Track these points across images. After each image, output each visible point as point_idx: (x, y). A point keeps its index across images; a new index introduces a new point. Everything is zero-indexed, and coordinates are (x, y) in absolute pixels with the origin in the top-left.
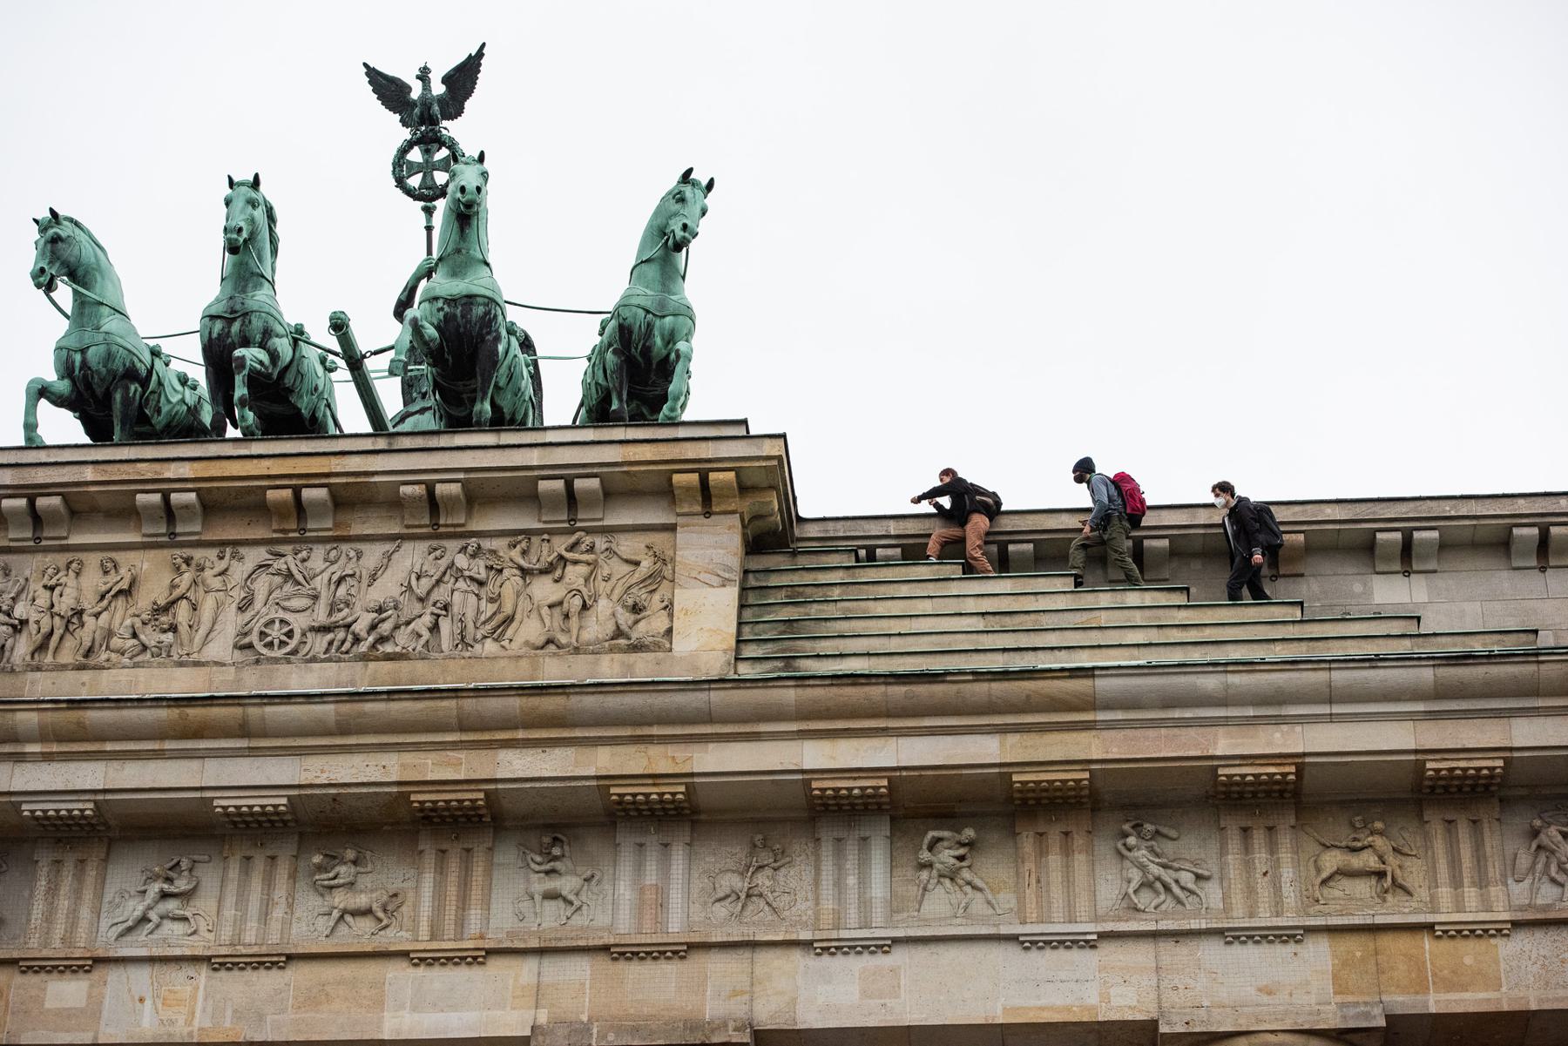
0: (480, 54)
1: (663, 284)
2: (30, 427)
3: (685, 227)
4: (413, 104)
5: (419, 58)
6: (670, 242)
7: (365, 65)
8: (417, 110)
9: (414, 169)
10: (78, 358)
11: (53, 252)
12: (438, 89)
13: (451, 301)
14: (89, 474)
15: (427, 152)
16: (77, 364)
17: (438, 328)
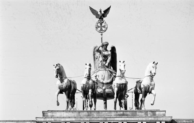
0: (110, 7)
1: (151, 81)
2: (57, 101)
3: (154, 73)
4: (99, 15)
5: (100, 8)
6: (152, 75)
7: (89, 7)
8: (99, 17)
9: (99, 27)
10: (61, 86)
11: (57, 71)
12: (103, 13)
13: (120, 85)
14: (74, 119)
15: (101, 24)
16: (61, 88)
17: (118, 88)
